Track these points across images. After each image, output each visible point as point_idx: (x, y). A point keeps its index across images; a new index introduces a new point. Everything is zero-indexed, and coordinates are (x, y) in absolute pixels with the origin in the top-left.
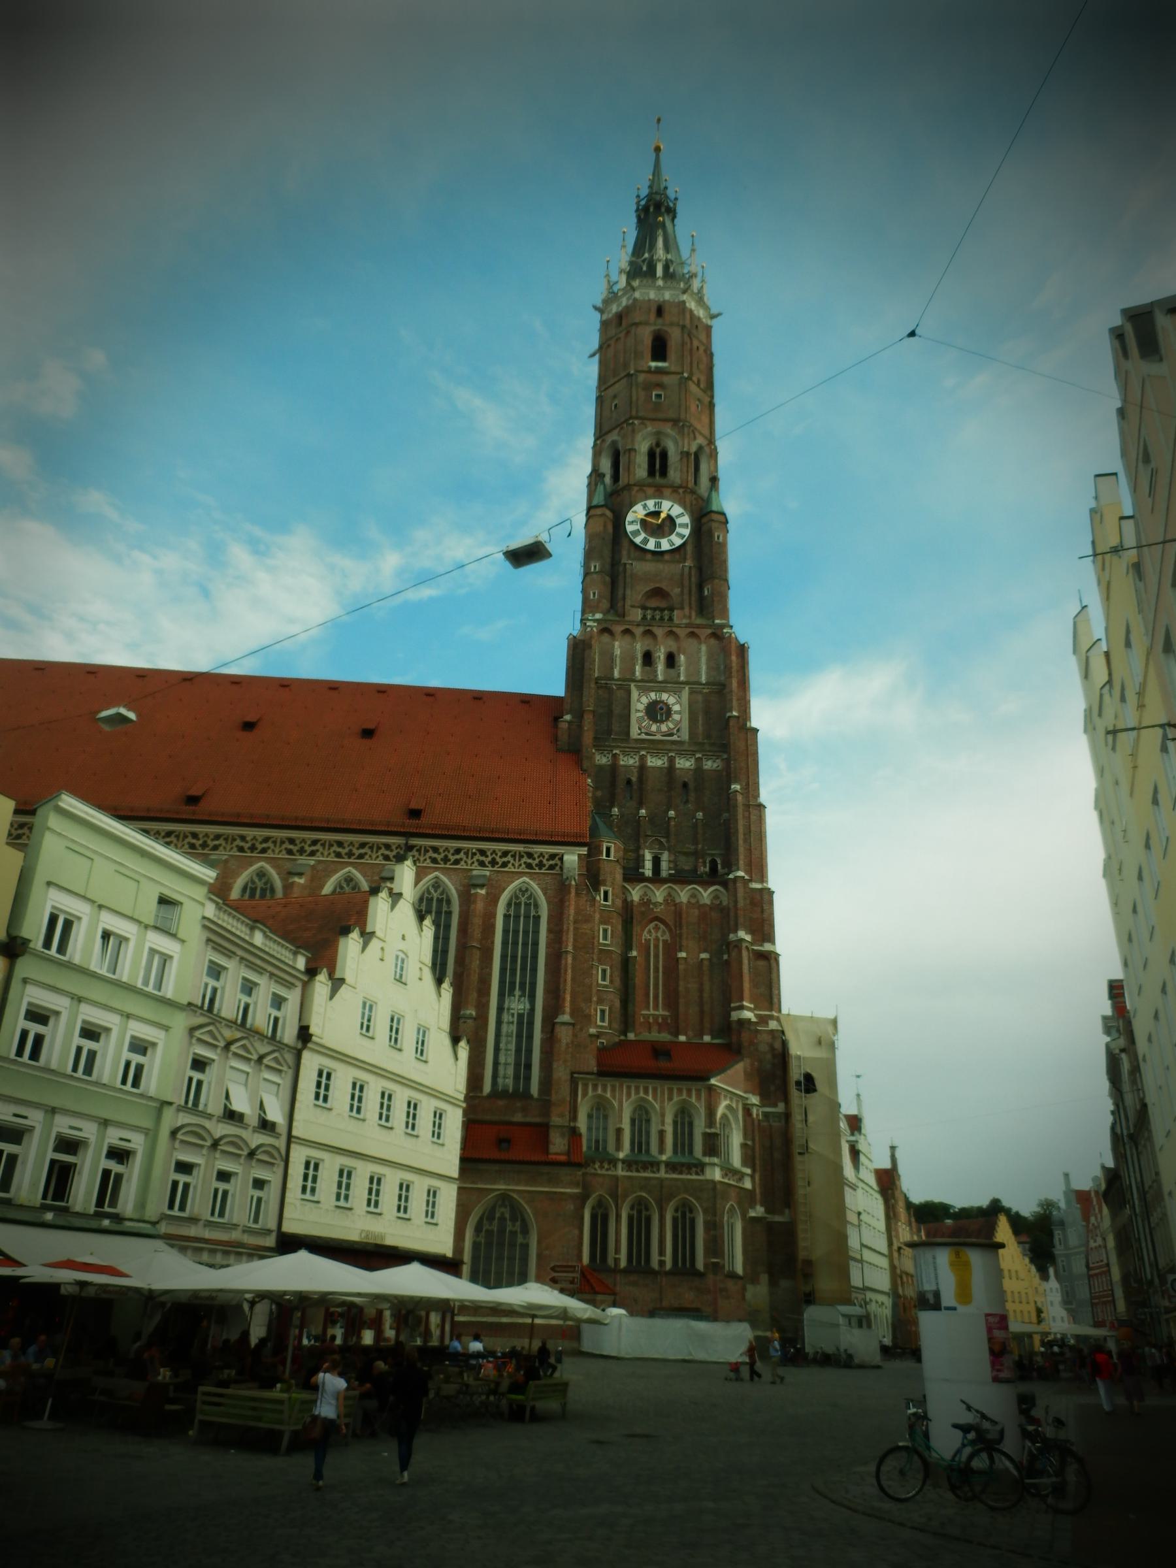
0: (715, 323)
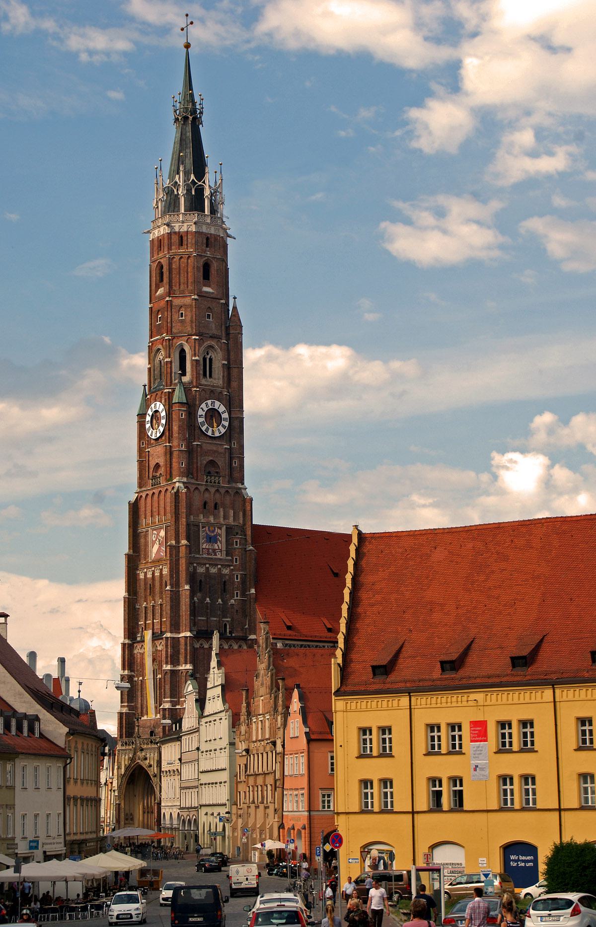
0: (229, 240)
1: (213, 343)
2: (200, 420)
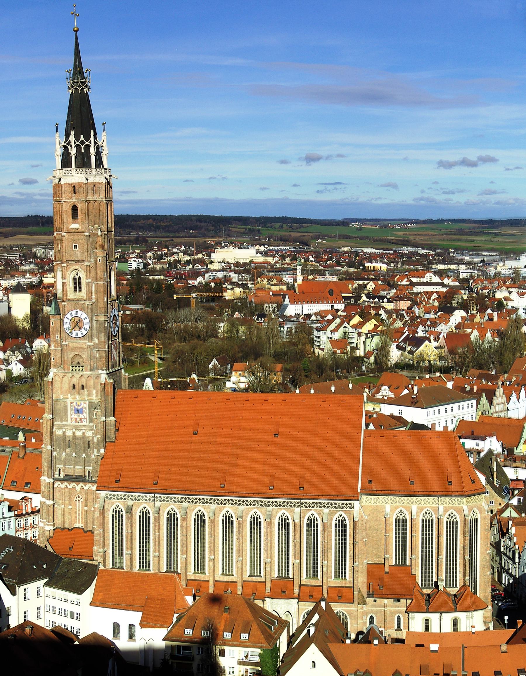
1: (77, 266)
2: (66, 326)
